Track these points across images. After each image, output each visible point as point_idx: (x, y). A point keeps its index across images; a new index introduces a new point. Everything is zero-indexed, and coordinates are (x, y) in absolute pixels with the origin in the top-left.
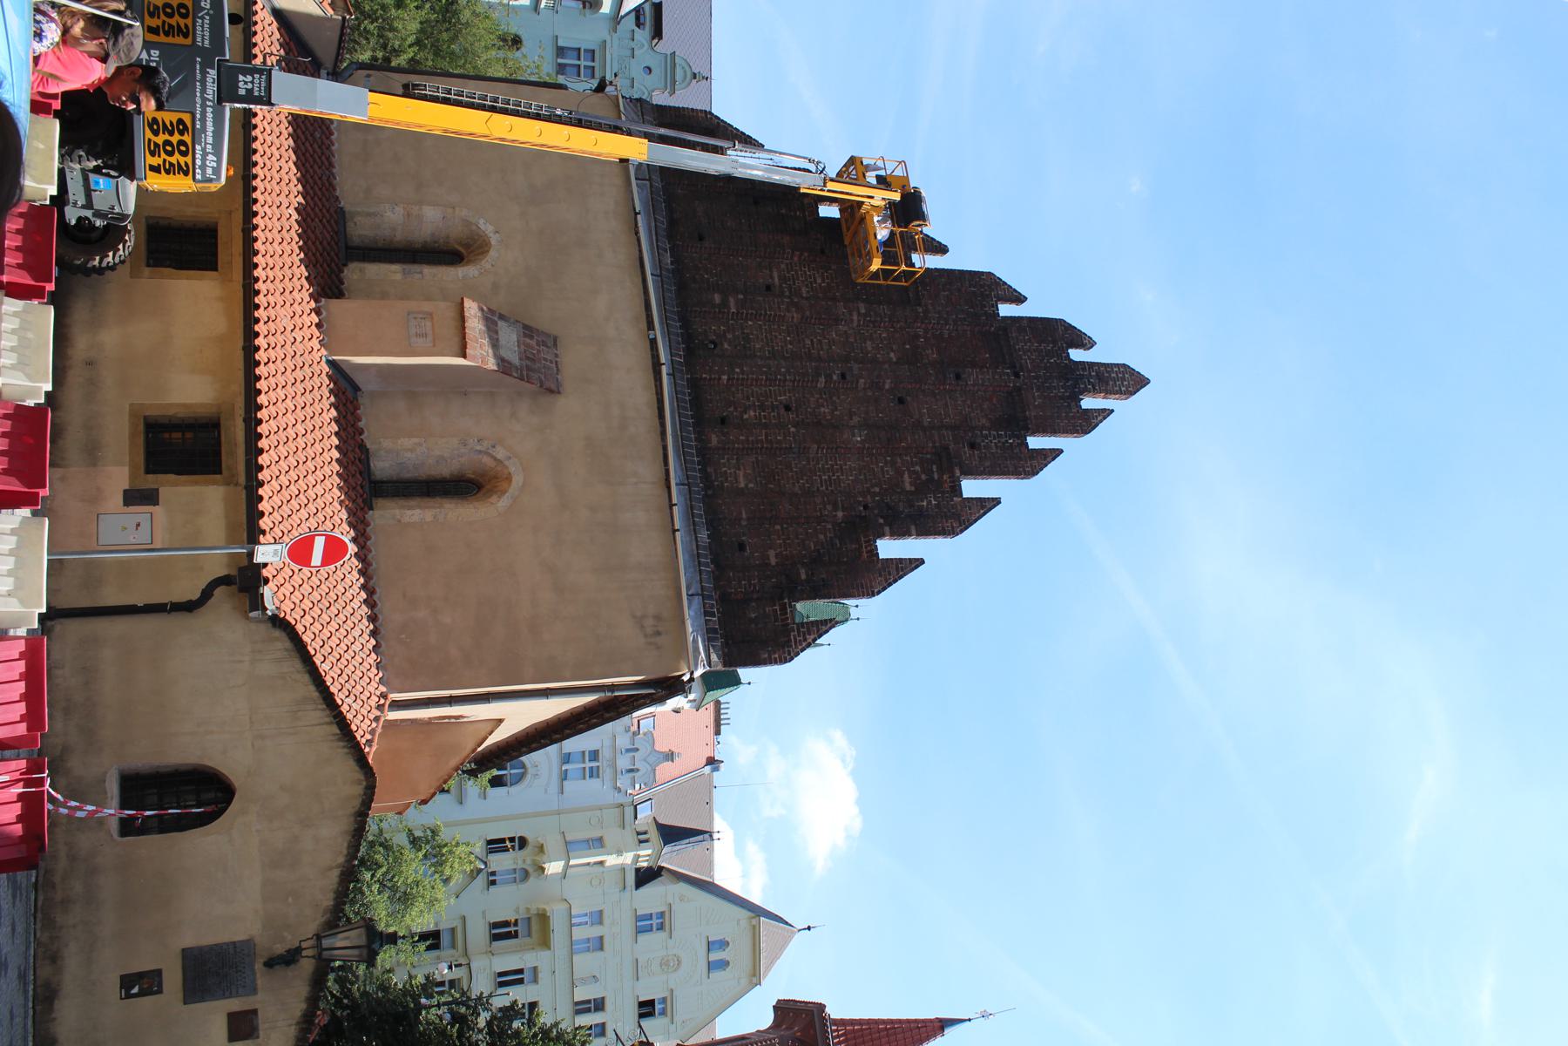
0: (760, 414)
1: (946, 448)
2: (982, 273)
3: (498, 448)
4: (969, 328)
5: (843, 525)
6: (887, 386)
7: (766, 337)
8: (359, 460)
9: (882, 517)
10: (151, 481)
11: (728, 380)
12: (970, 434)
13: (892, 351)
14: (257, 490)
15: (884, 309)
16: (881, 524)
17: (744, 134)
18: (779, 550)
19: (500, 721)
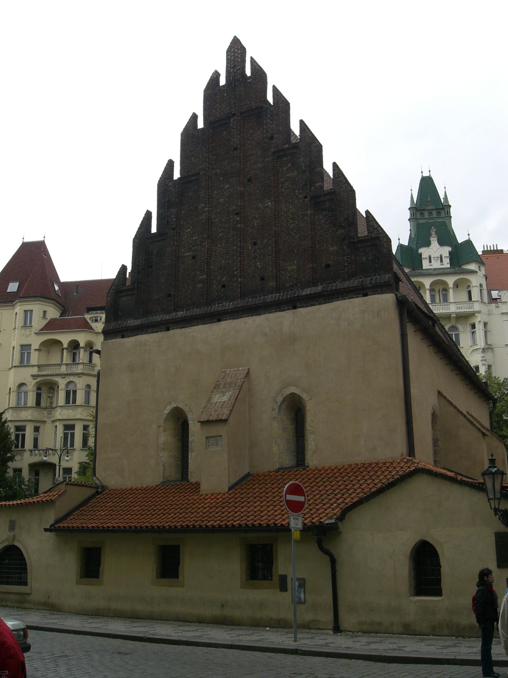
0: (259, 259)
1: (274, 153)
2: (182, 139)
3: (277, 400)
5: (316, 210)
6: (242, 189)
7: (219, 258)
8: (283, 473)
9: (310, 188)
10: (276, 579)
11: (241, 277)
12: (266, 140)
13: (224, 186)
14: (279, 526)
15: (202, 194)
16: (314, 189)
19: (439, 393)
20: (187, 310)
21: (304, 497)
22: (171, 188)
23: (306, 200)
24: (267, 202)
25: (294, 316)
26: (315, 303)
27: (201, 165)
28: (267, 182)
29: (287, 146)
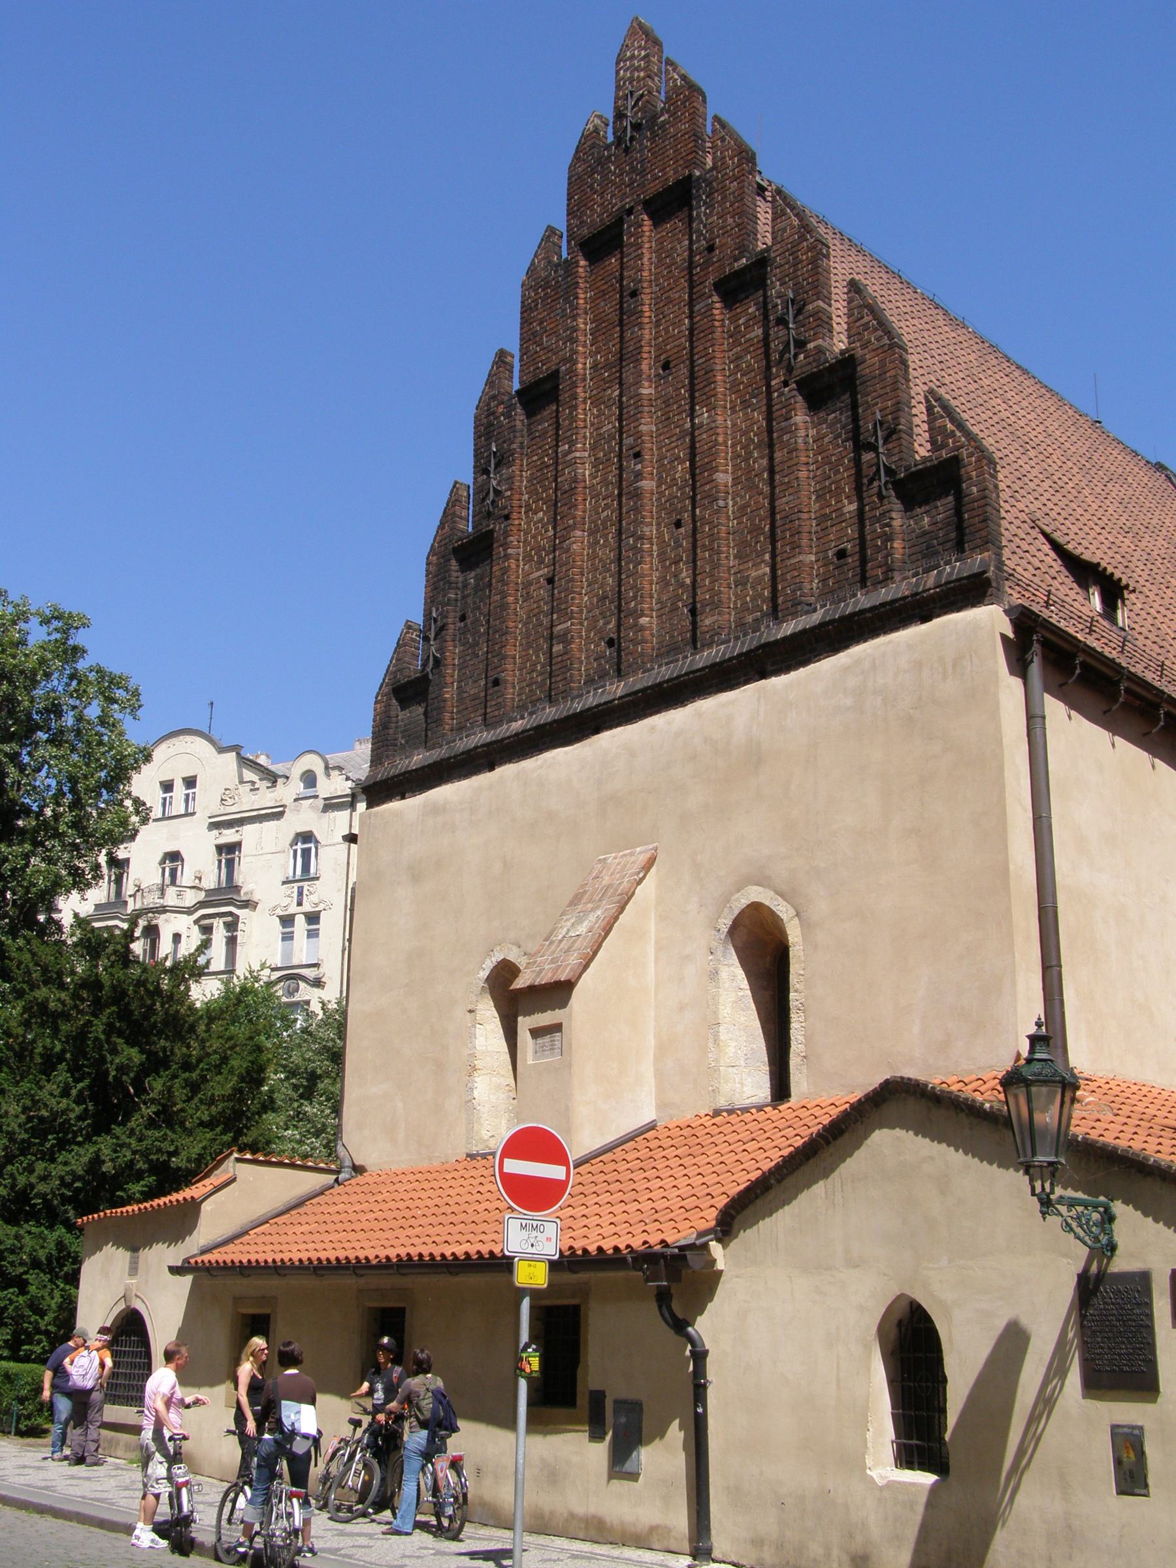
4: (582, 296)
9: (796, 356)
10: (583, 1400)
16: (805, 358)
17: (396, 649)
18: (846, 502)
20: (531, 714)
21: (564, 1168)
22: (502, 418)
23: (786, 389)
24: (700, 412)
25: (759, 700)
26: (808, 656)
27: (562, 350)
28: (700, 361)
29: (744, 260)
